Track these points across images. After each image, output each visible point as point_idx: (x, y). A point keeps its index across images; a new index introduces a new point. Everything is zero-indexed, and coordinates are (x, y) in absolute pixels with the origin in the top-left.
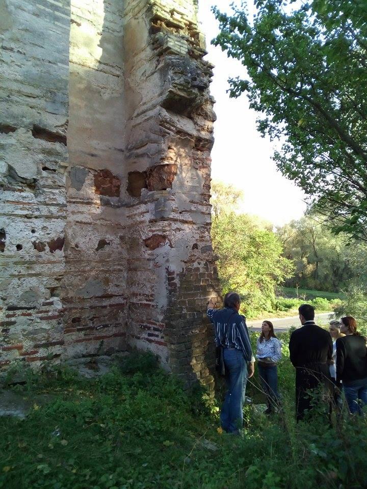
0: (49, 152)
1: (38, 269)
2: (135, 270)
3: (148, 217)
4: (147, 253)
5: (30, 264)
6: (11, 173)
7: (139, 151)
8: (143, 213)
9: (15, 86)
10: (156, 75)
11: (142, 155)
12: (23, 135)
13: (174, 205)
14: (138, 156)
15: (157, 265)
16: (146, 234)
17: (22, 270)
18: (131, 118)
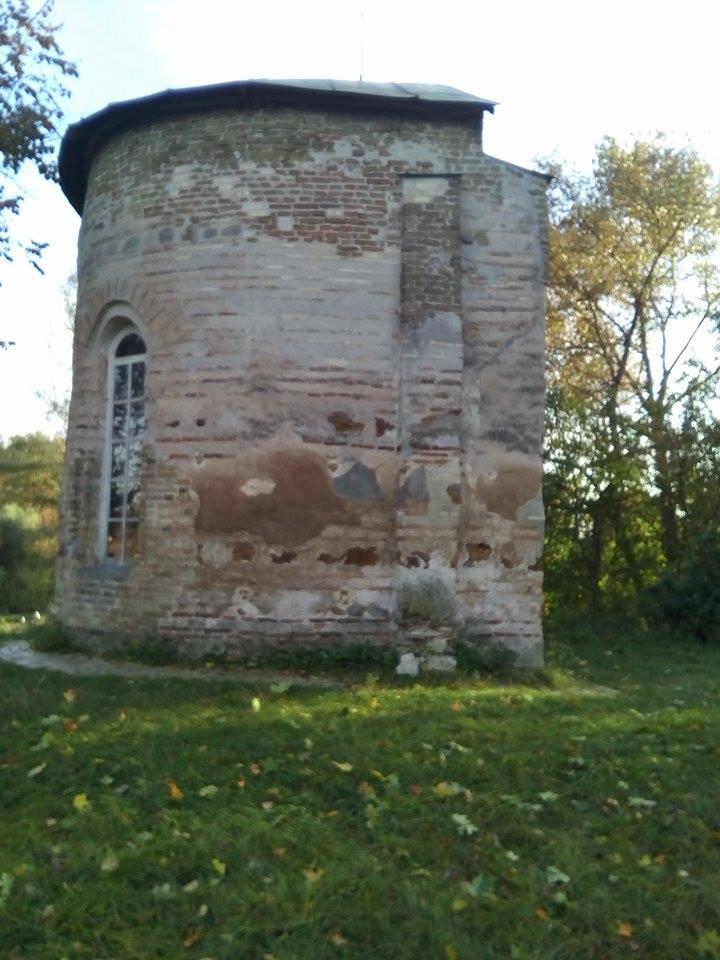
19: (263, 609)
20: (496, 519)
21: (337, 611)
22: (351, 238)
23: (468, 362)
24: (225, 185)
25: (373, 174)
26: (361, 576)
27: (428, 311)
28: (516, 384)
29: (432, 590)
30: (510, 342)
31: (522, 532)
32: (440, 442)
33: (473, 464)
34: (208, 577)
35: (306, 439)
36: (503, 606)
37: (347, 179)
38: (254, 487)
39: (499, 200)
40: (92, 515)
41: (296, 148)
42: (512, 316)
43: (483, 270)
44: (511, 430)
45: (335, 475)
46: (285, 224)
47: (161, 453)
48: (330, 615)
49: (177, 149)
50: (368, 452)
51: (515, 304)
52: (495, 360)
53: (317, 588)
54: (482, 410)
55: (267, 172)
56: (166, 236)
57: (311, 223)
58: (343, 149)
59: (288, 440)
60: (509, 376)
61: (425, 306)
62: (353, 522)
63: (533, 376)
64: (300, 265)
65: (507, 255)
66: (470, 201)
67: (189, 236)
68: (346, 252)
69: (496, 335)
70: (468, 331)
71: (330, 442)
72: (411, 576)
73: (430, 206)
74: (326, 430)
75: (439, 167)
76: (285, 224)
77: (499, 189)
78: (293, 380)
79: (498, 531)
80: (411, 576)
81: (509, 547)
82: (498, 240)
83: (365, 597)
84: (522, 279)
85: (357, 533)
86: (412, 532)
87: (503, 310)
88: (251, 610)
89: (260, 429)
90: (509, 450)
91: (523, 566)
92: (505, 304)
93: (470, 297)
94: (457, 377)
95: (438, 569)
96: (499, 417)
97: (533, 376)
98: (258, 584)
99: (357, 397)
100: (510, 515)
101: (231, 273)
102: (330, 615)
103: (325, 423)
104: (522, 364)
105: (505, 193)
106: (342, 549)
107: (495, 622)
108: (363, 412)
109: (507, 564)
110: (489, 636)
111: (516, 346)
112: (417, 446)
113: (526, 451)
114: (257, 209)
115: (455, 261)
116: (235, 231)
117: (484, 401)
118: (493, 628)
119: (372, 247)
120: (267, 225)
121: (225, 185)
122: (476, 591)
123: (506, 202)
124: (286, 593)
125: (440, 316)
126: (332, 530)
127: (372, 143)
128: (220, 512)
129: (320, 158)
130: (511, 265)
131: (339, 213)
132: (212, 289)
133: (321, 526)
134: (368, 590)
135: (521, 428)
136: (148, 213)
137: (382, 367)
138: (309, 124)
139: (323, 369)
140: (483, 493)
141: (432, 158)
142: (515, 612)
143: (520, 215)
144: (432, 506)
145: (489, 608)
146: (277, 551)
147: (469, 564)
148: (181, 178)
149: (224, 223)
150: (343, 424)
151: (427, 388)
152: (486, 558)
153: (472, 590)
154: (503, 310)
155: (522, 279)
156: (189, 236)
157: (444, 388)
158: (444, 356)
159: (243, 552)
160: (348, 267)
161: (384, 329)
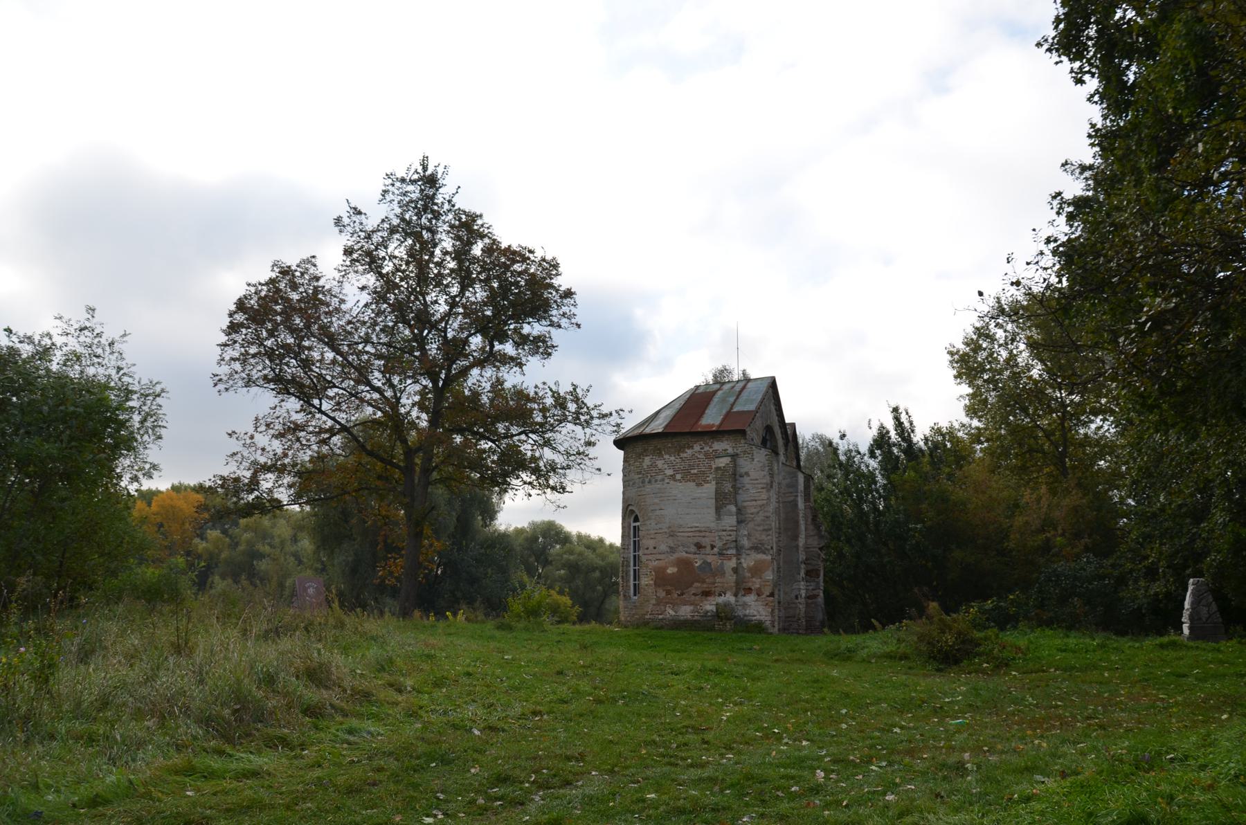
22: (699, 480)
23: (739, 522)
24: (660, 463)
25: (706, 454)
27: (725, 505)
29: (727, 605)
32: (729, 552)
34: (659, 602)
38: (670, 571)
40: (628, 581)
41: (681, 449)
42: (759, 503)
46: (678, 477)
47: (644, 559)
49: (645, 450)
52: (753, 520)
55: (673, 458)
56: (643, 482)
57: (687, 476)
58: (697, 448)
62: (704, 582)
64: (683, 490)
66: (741, 461)
67: (650, 482)
68: (699, 485)
70: (740, 511)
72: (721, 600)
74: (693, 549)
75: (730, 451)
76: (678, 477)
79: (756, 583)
80: (721, 600)
82: (753, 474)
83: (709, 608)
88: (672, 613)
89: (672, 550)
93: (740, 498)
95: (729, 598)
98: (674, 605)
106: (700, 591)
108: (706, 542)
114: (669, 472)
115: (734, 487)
117: (749, 536)
119: (708, 482)
120: (673, 477)
121: (660, 463)
126: (696, 584)
127: (706, 444)
128: (661, 579)
129: (689, 452)
132: (656, 501)
134: (709, 606)
136: (639, 473)
137: (713, 525)
138: (684, 441)
140: (750, 569)
141: (727, 447)
148: (647, 461)
149: (660, 477)
150: (699, 546)
156: (650, 482)
158: (730, 521)
159: (668, 592)
160: (699, 490)
161: (713, 511)
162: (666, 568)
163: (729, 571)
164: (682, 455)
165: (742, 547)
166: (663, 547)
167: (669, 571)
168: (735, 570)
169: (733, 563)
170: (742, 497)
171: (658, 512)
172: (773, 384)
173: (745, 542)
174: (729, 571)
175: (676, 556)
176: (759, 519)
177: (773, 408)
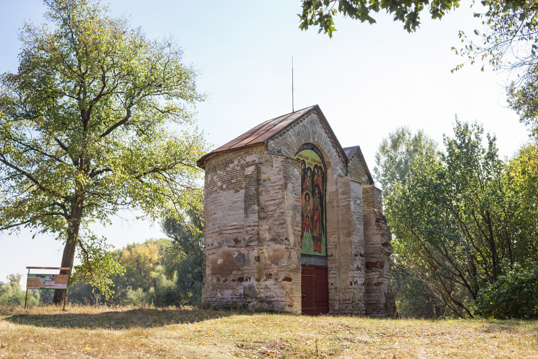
0: (362, 260)
1: (362, 291)
2: (371, 293)
3: (376, 276)
4: (376, 288)
5: (360, 289)
6: (357, 267)
7: (372, 256)
8: (375, 275)
9: (357, 244)
10: (379, 236)
11: (373, 257)
12: (359, 256)
13: (385, 273)
14: (371, 257)
15: (380, 291)
16: (375, 281)
17: (359, 291)
18: (366, 244)
19: (222, 295)
20: (273, 266)
21: (236, 295)
26: (241, 285)
27: (250, 205)
28: (278, 223)
29: (251, 288)
30: (276, 210)
31: (280, 269)
32: (252, 244)
33: (267, 249)
35: (229, 246)
36: (275, 293)
37: (237, 170)
39: (272, 166)
42: (277, 201)
43: (269, 189)
44: (277, 237)
45: (235, 256)
48: (234, 296)
50: (242, 248)
51: (278, 197)
53: (232, 289)
54: (269, 232)
55: (222, 173)
59: (225, 248)
60: (276, 220)
61: (249, 204)
63: (282, 219)
65: (275, 182)
66: (263, 168)
69: (273, 208)
71: (234, 247)
73: (251, 175)
74: (233, 243)
77: (272, 163)
78: (227, 230)
81: (277, 274)
82: (273, 179)
84: (279, 189)
85: (240, 273)
86: (246, 271)
87: (274, 200)
89: (220, 245)
90: (276, 244)
91: (280, 280)
92: (275, 198)
94: (257, 224)
95: (253, 282)
96: (274, 234)
97: (282, 219)
99: (240, 233)
100: (277, 264)
101: (216, 202)
102: (234, 296)
103: (233, 242)
104: (279, 216)
105: (274, 164)
106: (237, 278)
107: (274, 297)
109: (276, 279)
110: (272, 301)
111: (277, 211)
112: (247, 246)
113: (280, 244)
114: (219, 184)
115: (257, 189)
116: (216, 190)
117: (270, 230)
118: (273, 299)
122: (268, 288)
123: (274, 166)
124: (225, 290)
125: (253, 207)
130: (276, 186)
131: (234, 181)
133: (232, 271)
135: (279, 236)
137: (243, 223)
139: (232, 226)
142: (279, 294)
143: (278, 169)
144: (251, 263)
145: (272, 293)
146: (224, 279)
147: (266, 280)
150: (237, 241)
151: (250, 228)
152: (271, 278)
153: (266, 287)
154: (274, 200)
155: (279, 189)
157: (253, 228)
158: (254, 218)
160: (237, 195)
162: (216, 260)
163: (252, 260)
164: (228, 169)
165: (264, 240)
166: (216, 244)
167: (219, 263)
168: (258, 259)
169: (254, 253)
170: (263, 198)
171: (214, 216)
172: (316, 109)
173: (267, 236)
174: (252, 260)
175: (222, 249)
176: (276, 215)
177: (322, 131)
